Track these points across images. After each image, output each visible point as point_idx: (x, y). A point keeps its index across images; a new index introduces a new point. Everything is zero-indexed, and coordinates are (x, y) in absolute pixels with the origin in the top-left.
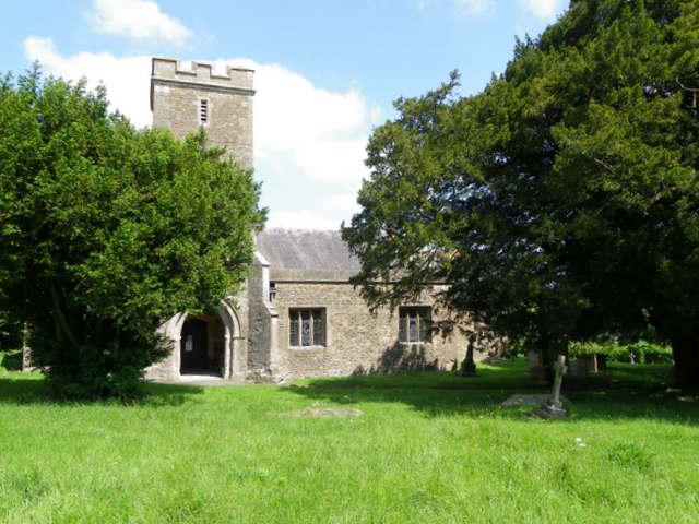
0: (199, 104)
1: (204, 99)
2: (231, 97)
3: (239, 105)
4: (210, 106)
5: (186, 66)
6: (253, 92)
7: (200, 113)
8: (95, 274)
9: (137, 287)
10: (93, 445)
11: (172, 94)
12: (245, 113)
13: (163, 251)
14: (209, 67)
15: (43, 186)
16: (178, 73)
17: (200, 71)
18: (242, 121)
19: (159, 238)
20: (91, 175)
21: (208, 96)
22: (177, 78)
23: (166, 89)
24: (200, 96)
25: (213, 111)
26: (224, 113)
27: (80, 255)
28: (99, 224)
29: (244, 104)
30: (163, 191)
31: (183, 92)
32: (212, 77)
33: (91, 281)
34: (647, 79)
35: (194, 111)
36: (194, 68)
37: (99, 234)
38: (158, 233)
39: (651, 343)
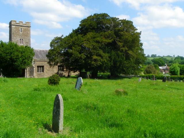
0: (20, 29)
1: (21, 28)
2: (27, 28)
3: (28, 29)
4: (22, 29)
5: (17, 22)
6: (30, 27)
7: (20, 31)
8: (17, 64)
9: (21, 65)
10: (13, 83)
11: (15, 27)
12: (29, 31)
13: (24, 61)
14: (22, 22)
15: (12, 55)
16: (16, 23)
17: (20, 23)
18: (28, 32)
19: (24, 59)
20: (16, 53)
21: (22, 27)
22: (16, 24)
23: (14, 26)
24: (20, 28)
25: (23, 31)
26: (25, 30)
27: (15, 62)
28: (17, 59)
29: (29, 29)
30: (23, 54)
31: (17, 27)
32: (23, 24)
33: (16, 65)
34: (100, 29)
35: (19, 30)
36: (19, 22)
37: (17, 60)
38: (23, 59)
39: (104, 72)
